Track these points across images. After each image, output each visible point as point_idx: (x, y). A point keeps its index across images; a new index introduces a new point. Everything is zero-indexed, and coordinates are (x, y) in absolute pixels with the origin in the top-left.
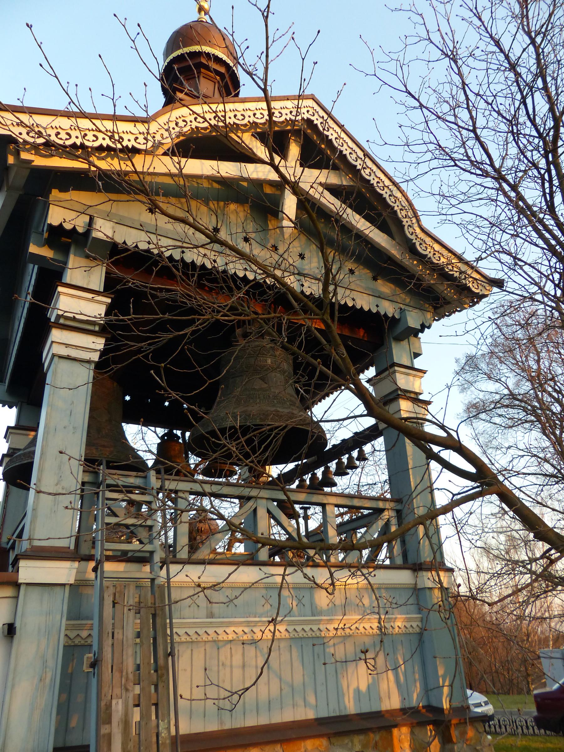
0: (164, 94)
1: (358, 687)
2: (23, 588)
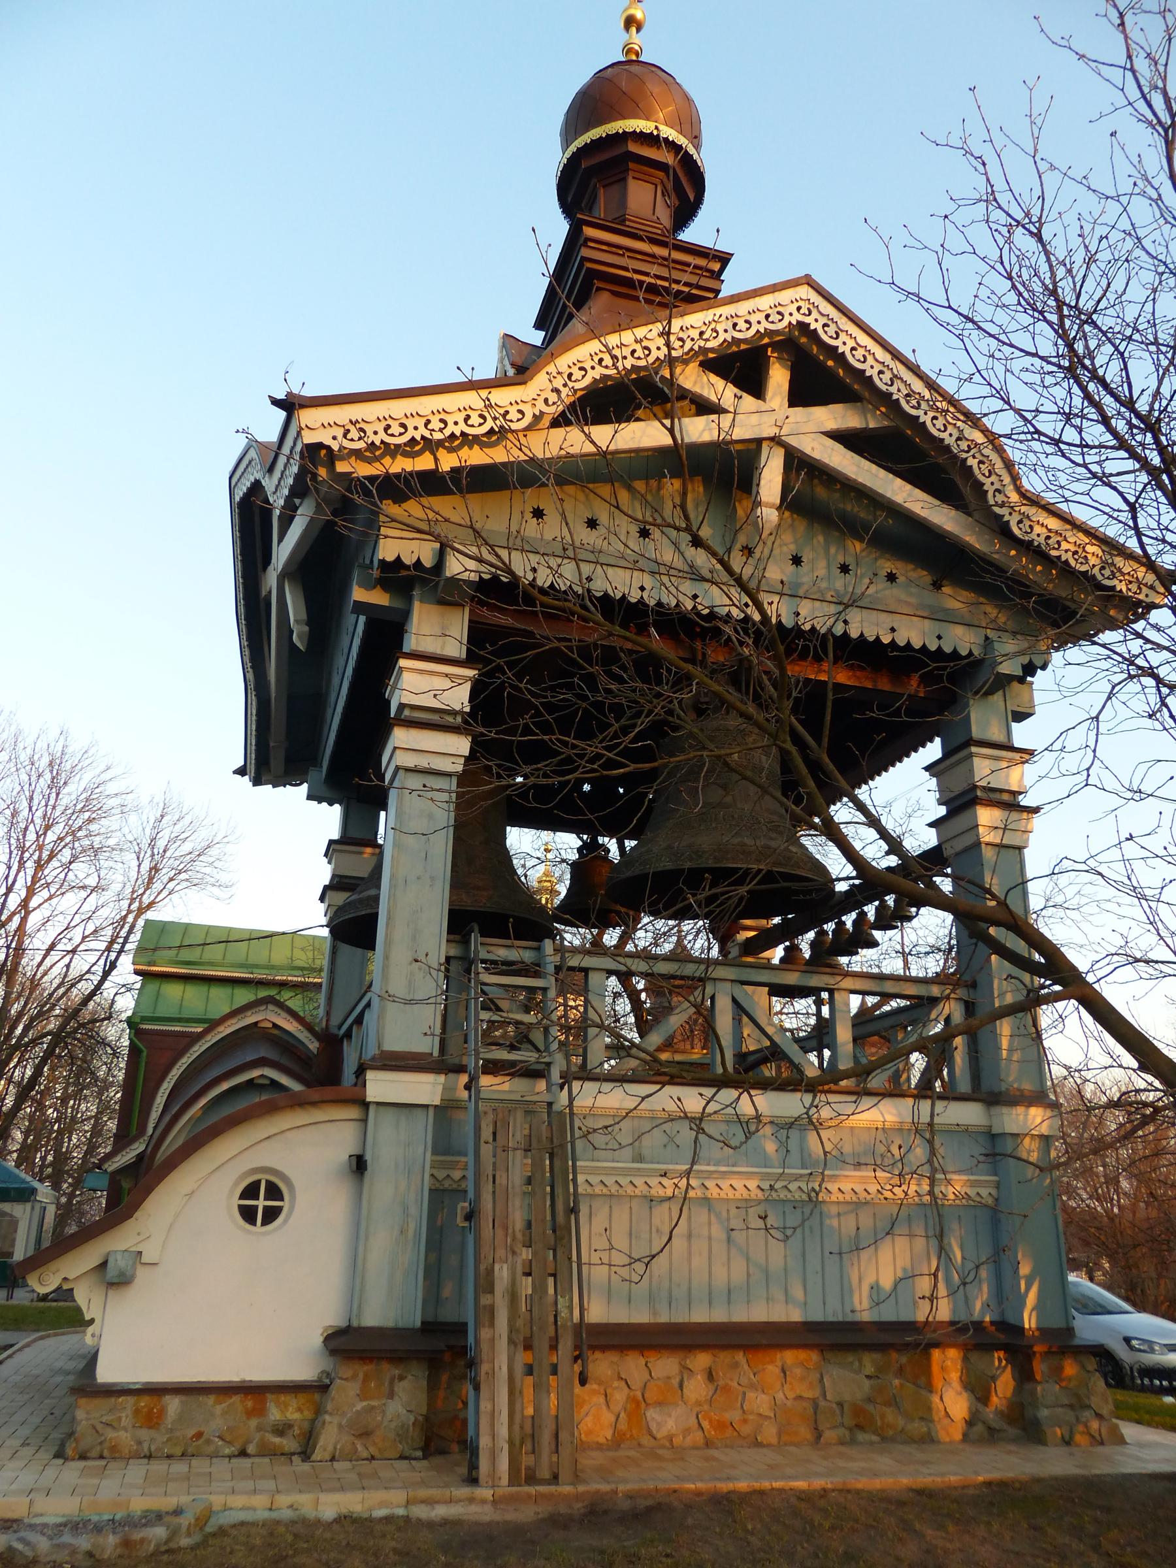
0: (563, 212)
1: (877, 1282)
2: (372, 1109)
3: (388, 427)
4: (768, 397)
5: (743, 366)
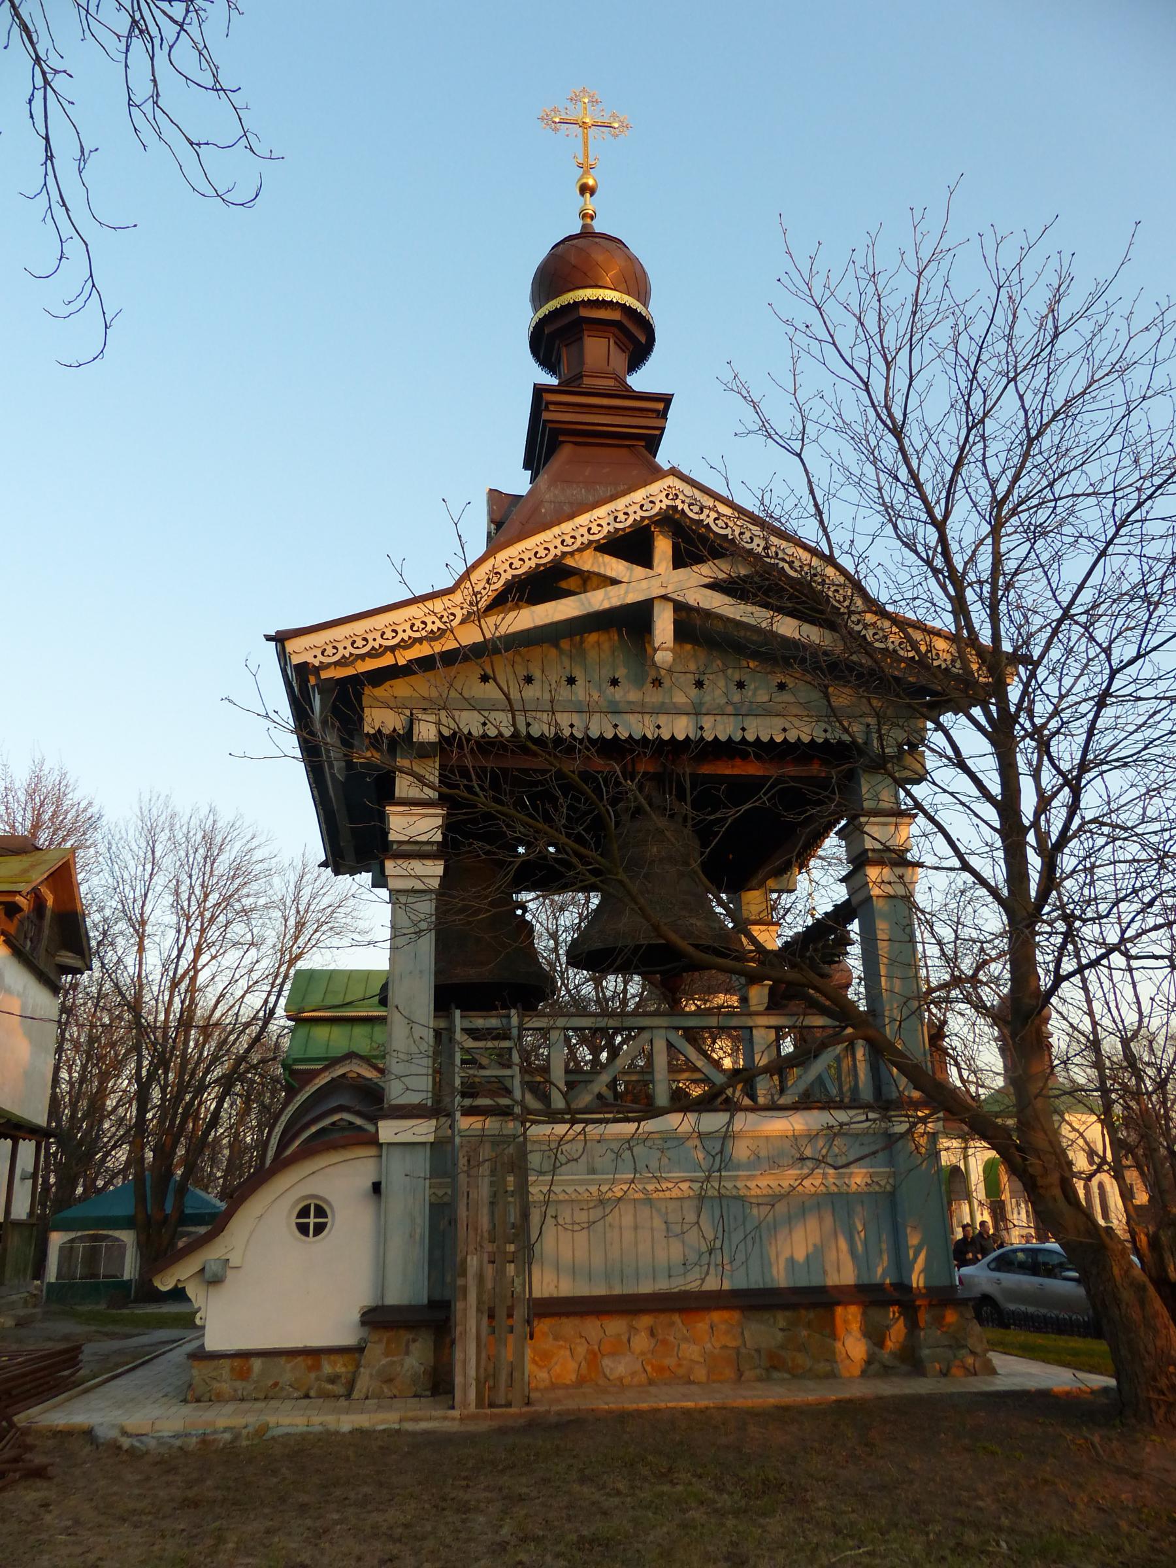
0: (540, 365)
1: (792, 1258)
2: (384, 1148)
3: (354, 642)
5: (632, 545)
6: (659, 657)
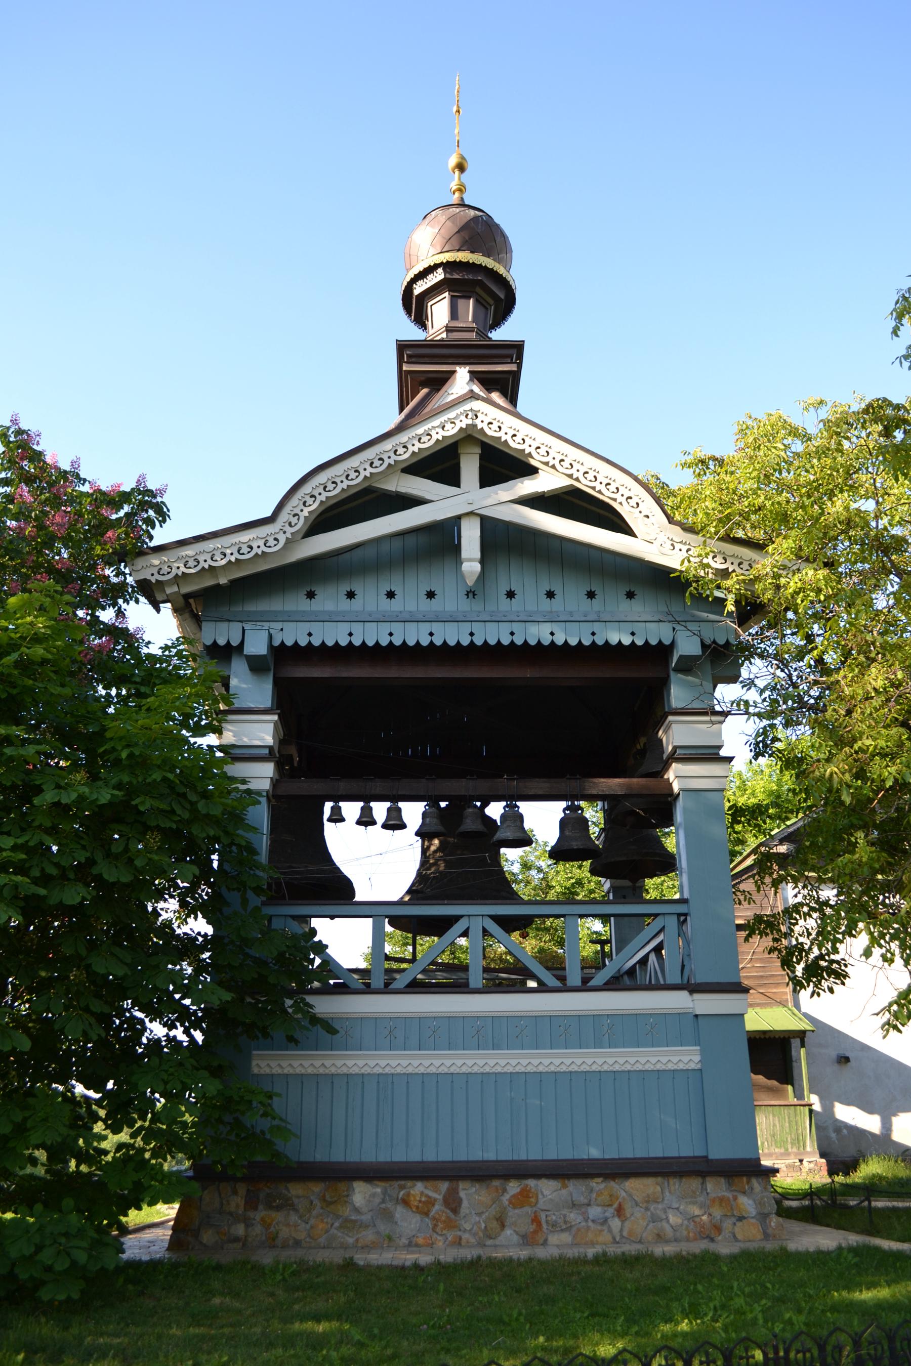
4: (462, 485)
6: (466, 567)
